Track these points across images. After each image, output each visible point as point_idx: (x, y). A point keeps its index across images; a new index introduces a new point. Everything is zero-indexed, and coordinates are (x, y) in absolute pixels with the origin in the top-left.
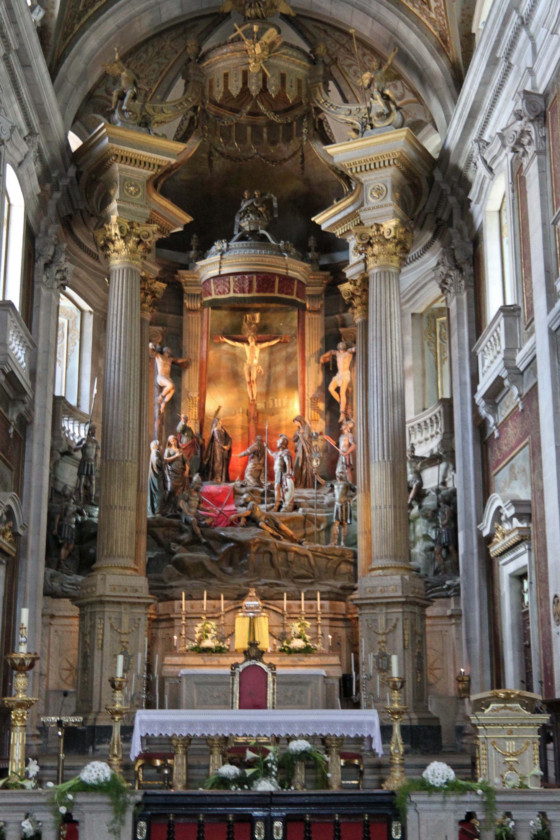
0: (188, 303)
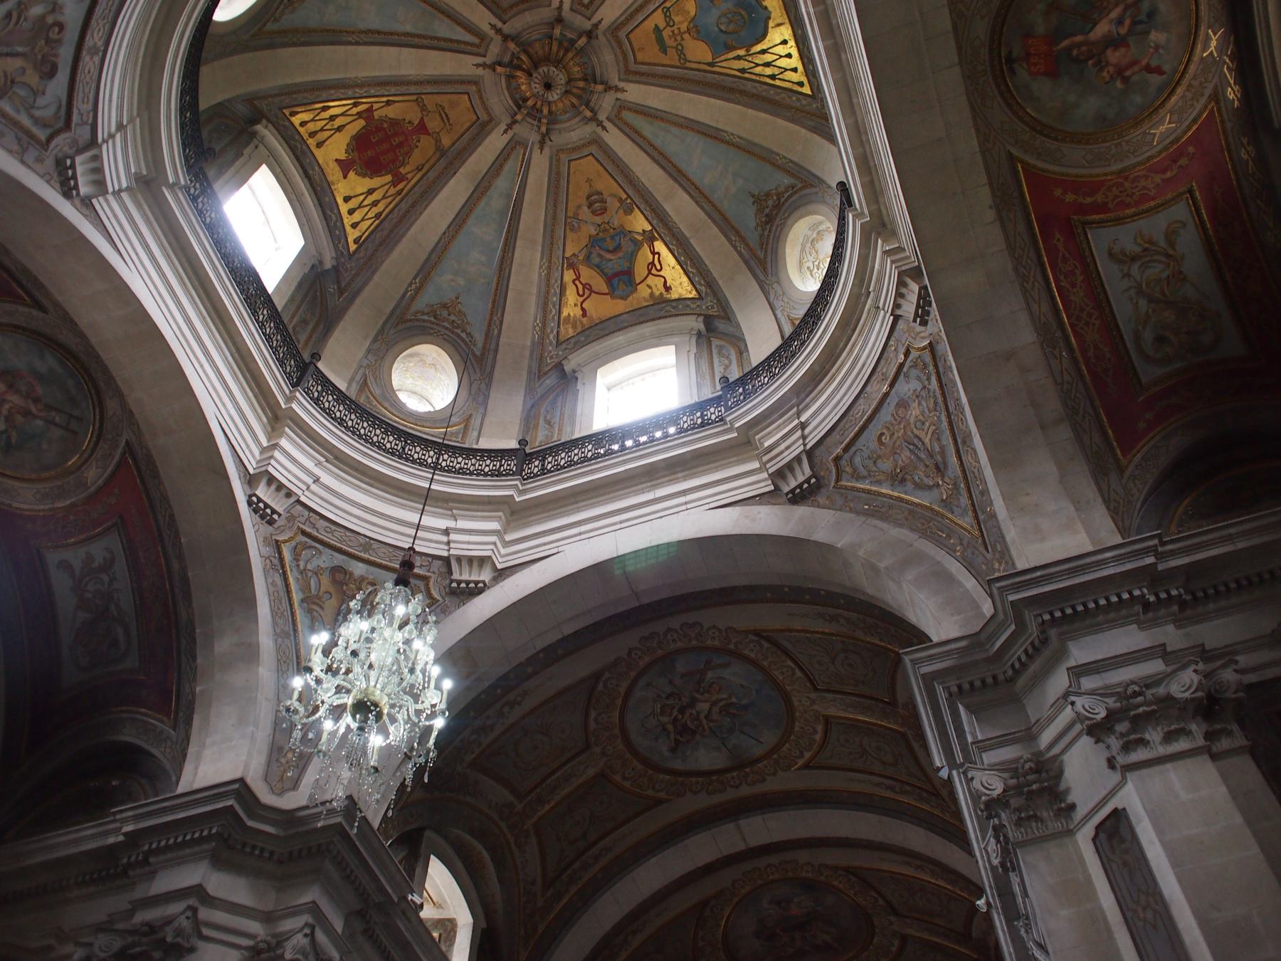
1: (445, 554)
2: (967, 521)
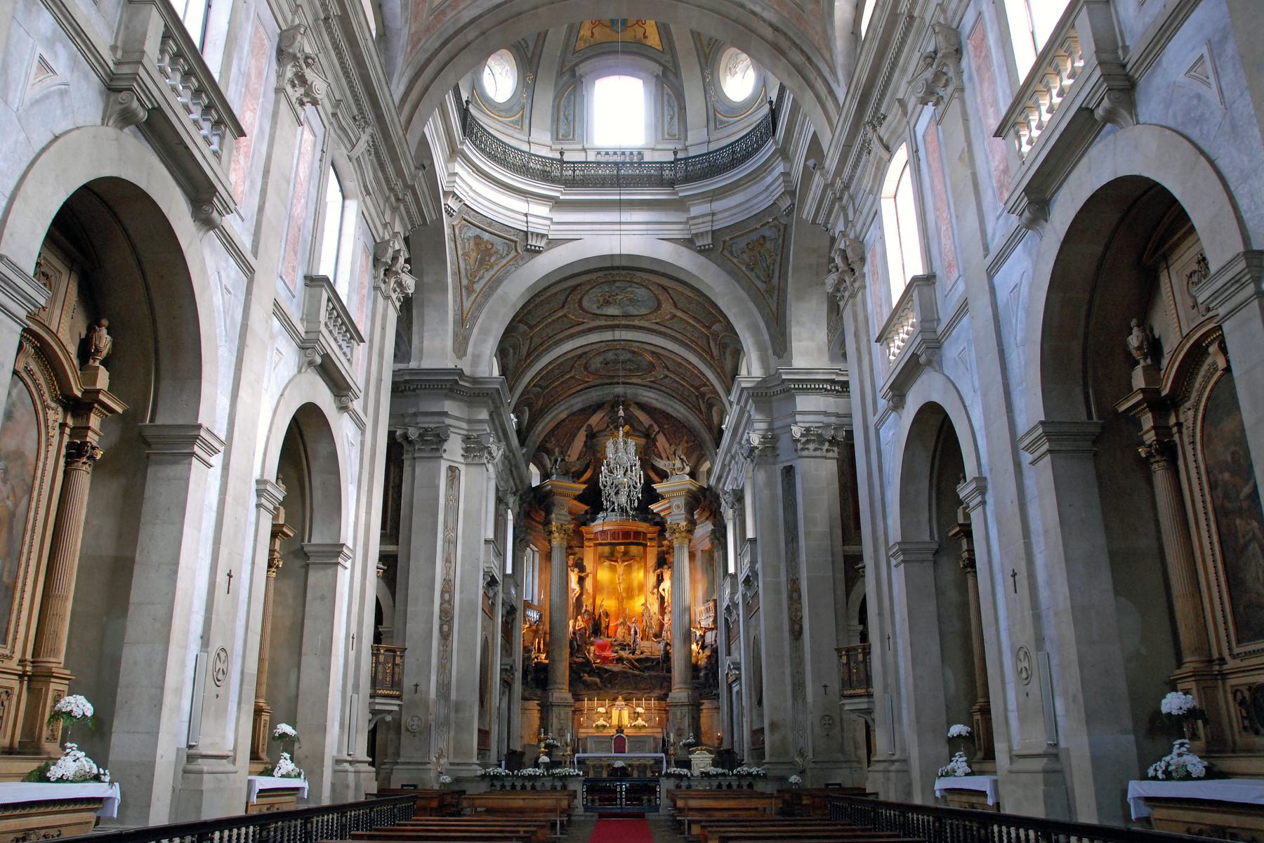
0: (586, 543)
1: (525, 229)
2: (774, 309)
